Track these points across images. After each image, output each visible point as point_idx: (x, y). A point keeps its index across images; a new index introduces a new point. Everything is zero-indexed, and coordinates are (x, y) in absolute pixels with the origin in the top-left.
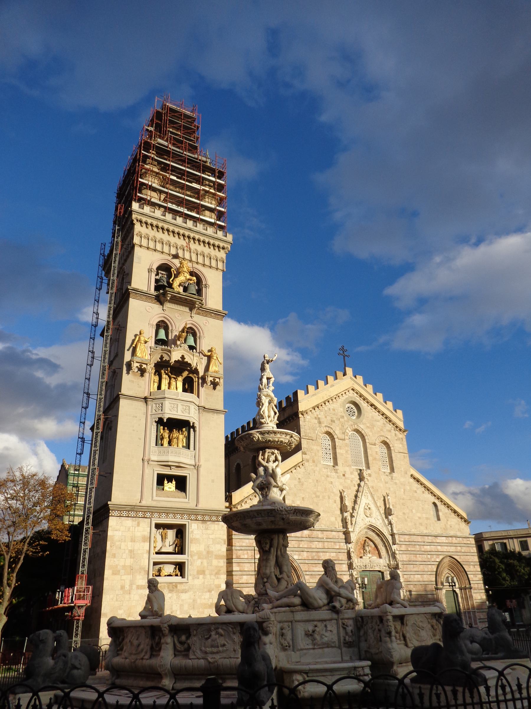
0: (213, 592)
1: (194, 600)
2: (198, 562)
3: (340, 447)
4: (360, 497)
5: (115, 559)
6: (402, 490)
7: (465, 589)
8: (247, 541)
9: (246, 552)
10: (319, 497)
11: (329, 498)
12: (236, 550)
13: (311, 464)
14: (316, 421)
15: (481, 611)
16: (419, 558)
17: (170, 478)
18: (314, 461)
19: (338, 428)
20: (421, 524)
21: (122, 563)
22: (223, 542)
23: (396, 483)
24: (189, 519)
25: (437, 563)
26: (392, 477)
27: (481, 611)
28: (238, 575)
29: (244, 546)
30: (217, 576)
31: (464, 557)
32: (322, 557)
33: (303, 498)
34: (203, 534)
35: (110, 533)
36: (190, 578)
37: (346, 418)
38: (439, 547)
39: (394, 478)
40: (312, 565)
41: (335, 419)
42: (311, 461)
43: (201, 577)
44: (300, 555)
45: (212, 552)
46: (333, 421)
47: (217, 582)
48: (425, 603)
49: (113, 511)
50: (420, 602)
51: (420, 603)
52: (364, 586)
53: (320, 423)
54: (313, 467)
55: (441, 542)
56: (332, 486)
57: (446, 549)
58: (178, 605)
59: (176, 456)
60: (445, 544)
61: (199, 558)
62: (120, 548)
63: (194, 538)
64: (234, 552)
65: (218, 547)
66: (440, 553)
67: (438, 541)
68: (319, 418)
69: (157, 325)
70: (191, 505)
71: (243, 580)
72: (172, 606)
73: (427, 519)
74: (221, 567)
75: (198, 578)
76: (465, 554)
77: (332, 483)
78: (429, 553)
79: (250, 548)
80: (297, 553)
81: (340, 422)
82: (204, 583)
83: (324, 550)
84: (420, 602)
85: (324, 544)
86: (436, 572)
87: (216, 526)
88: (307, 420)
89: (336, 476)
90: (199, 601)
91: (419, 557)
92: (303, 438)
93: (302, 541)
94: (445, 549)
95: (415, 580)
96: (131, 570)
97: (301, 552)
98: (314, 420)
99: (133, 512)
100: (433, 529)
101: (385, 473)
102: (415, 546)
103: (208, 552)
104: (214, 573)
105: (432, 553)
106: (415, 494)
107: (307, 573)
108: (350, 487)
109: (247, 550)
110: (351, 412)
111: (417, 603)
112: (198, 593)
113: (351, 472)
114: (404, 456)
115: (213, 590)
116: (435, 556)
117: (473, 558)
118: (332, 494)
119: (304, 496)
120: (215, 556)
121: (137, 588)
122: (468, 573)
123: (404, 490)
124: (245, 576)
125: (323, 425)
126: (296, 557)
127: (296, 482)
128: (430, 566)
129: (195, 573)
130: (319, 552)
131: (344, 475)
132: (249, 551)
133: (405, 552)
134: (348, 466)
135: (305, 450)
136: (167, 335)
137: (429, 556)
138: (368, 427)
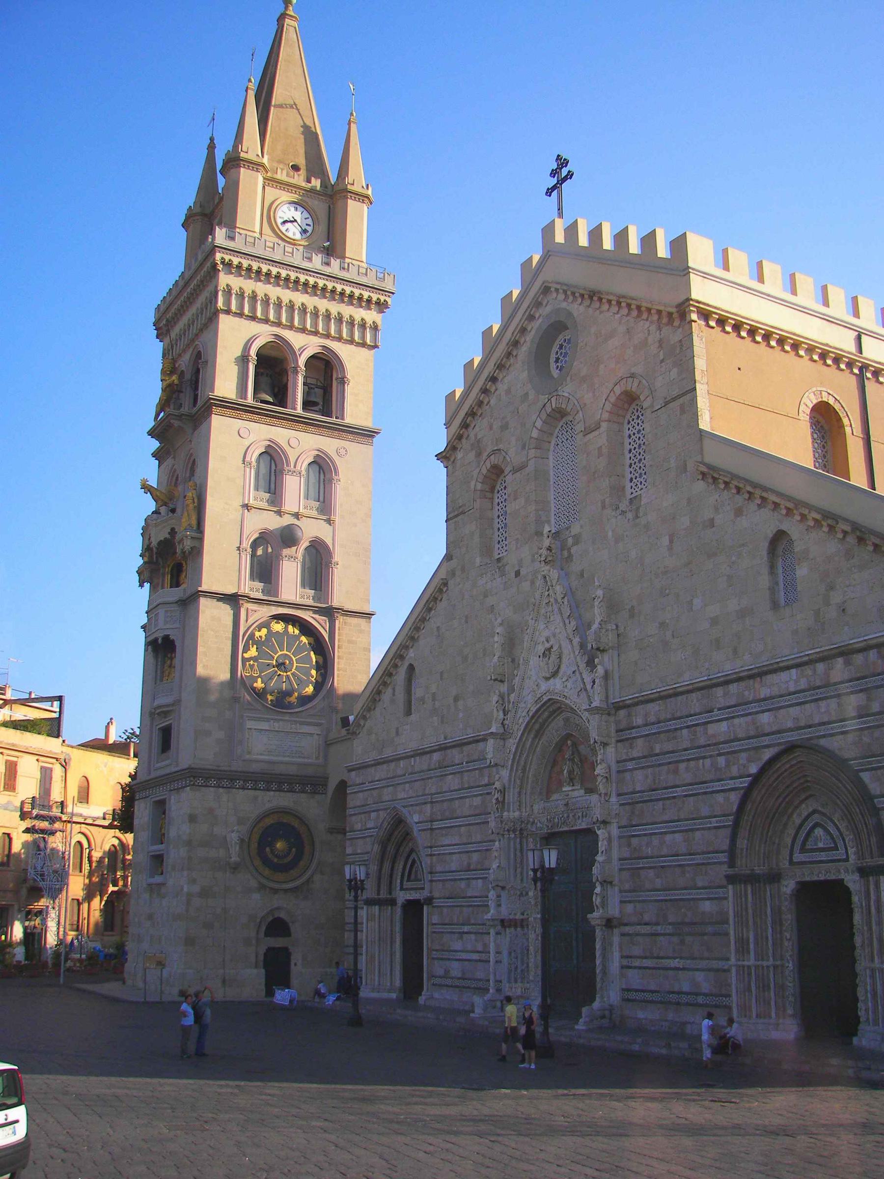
6: (665, 541)
8: (361, 795)
14: (474, 452)
18: (463, 569)
19: (513, 439)
20: (717, 644)
25: (745, 782)
26: (638, 509)
38: (765, 718)
50: (670, 924)
51: (670, 929)
55: (775, 691)
57: (796, 719)
60: (793, 699)
66: (766, 741)
67: (764, 692)
68: (479, 441)
78: (726, 748)
80: (418, 808)
83: (463, 793)
84: (670, 924)
88: (458, 463)
91: (687, 768)
94: (789, 717)
95: (665, 851)
102: (679, 733)
111: (659, 929)
116: (744, 755)
123: (671, 541)
125: (485, 455)
131: (517, 574)
133: (644, 763)
137: (721, 761)
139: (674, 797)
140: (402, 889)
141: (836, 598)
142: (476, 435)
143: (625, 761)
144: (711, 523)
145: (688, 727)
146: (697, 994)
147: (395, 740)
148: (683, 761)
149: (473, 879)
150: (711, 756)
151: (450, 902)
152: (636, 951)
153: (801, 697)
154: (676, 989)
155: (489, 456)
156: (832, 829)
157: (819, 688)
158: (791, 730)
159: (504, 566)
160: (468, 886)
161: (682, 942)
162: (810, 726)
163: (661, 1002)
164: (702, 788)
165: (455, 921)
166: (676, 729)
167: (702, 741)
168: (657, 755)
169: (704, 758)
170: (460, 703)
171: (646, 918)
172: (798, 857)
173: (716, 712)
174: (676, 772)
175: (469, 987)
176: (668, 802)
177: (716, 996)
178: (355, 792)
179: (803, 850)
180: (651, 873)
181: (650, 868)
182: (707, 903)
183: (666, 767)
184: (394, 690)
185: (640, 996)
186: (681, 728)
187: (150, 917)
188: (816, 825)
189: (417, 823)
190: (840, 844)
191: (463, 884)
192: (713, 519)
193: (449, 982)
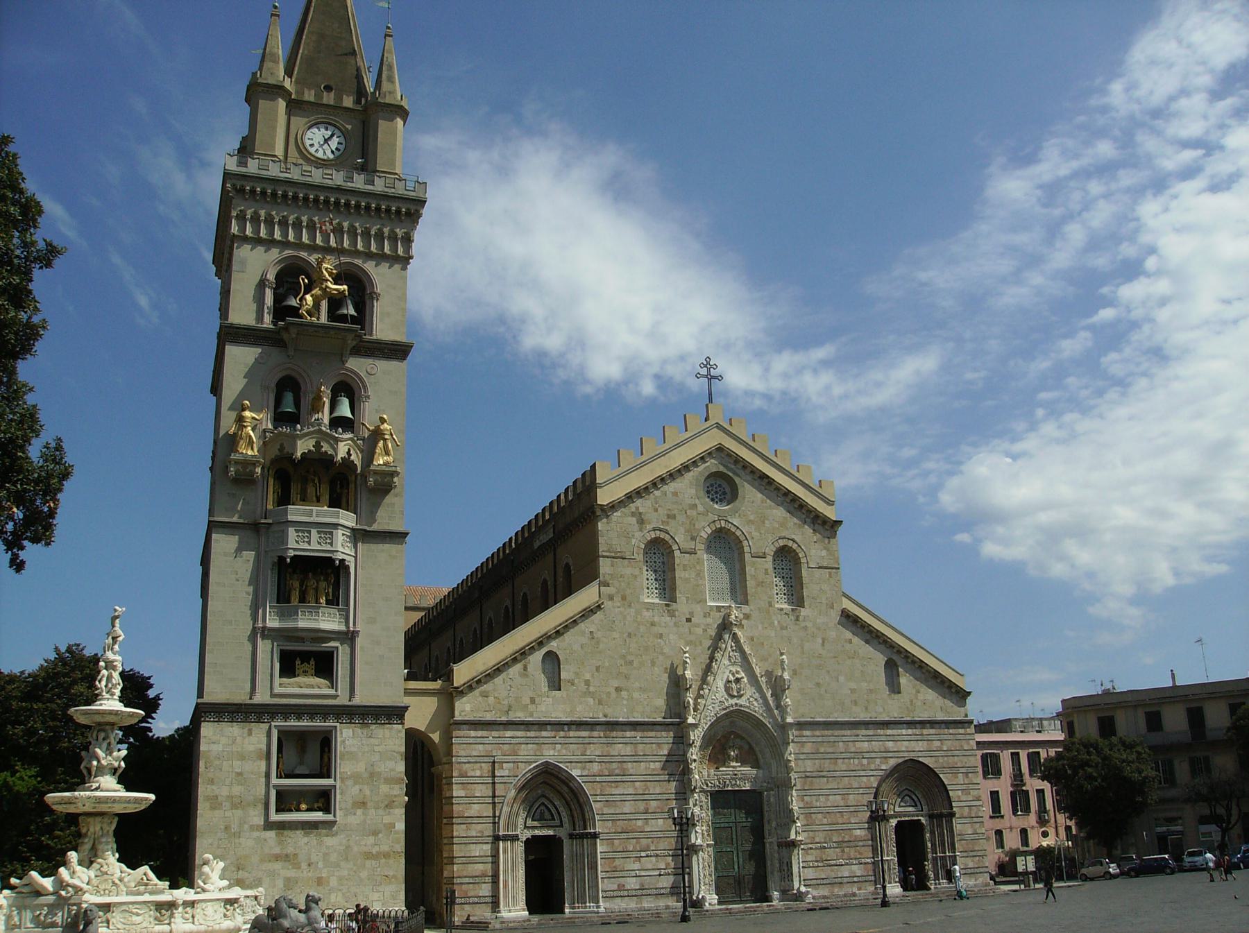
0: (380, 835)
1: (348, 847)
2: (355, 790)
3: (684, 566)
4: (719, 660)
5: (214, 787)
7: (941, 816)
9: (479, 765)
10: (631, 663)
11: (653, 663)
12: (460, 763)
13: (619, 604)
15: (971, 854)
16: (841, 765)
17: (305, 656)
18: (624, 598)
19: (682, 530)
21: (225, 792)
22: (399, 757)
23: (805, 628)
24: (338, 722)
27: (971, 854)
28: (462, 803)
29: (475, 756)
30: (388, 810)
31: (946, 758)
32: (631, 771)
33: (598, 669)
34: (362, 744)
35: (203, 747)
36: (338, 813)
37: (700, 508)
38: (890, 744)
39: (801, 618)
40: (609, 784)
41: (676, 512)
42: (617, 599)
43: (359, 812)
44: (584, 768)
45: (380, 773)
46: (671, 517)
47: (387, 819)
48: (845, 844)
49: (207, 714)
52: (684, 820)
53: (641, 522)
54: (622, 609)
56: (663, 643)
57: (907, 747)
58: (321, 854)
59: (311, 619)
61: (355, 783)
62: (221, 769)
63: (347, 752)
64: (455, 766)
65: (391, 764)
66: (890, 754)
68: (640, 513)
69: (277, 385)
70: (343, 700)
71: (473, 812)
72: (310, 855)
73: (871, 691)
74: (395, 796)
75: (355, 814)
76: (950, 753)
77: (661, 636)
79: (486, 759)
80: (580, 764)
81: (687, 516)
82: (365, 821)
83: (636, 758)
85: (636, 748)
86: (877, 789)
87: (387, 732)
89: (672, 624)
90: (356, 849)
92: (603, 557)
93: (590, 743)
96: (237, 803)
97: (588, 764)
98: (630, 518)
99: (240, 714)
100: (881, 710)
101: (782, 609)
102: (836, 744)
103: (372, 775)
104: (383, 805)
105: (873, 755)
106: (848, 646)
107: (598, 798)
108: (701, 642)
109: (480, 762)
110: (716, 493)
112: (353, 836)
113: (705, 613)
114: (830, 573)
115: (380, 832)
116: (878, 760)
117: (966, 760)
118: (661, 658)
119: (599, 663)
120: (385, 779)
121: (251, 828)
122: (949, 788)
123: (823, 642)
124: (476, 805)
125: (649, 527)
126: (575, 773)
127: (584, 640)
128: (864, 779)
129: (349, 806)
130: (625, 762)
131: (689, 620)
132: (483, 765)
133: (812, 756)
134: (698, 603)
135: (608, 578)
136: (297, 404)
137: (865, 761)
138: (750, 522)
139: (834, 777)
140: (525, 827)
141: (921, 697)
142: (637, 508)
143: (799, 754)
144: (850, 641)
145: (843, 741)
146: (854, 877)
147: (529, 706)
148: (840, 758)
149: (653, 819)
150: (858, 758)
151: (624, 836)
152: (809, 858)
153: (909, 738)
154: (840, 876)
155: (654, 530)
156: (914, 797)
157: (918, 735)
158: (903, 751)
159: (674, 611)
160: (647, 824)
161: (843, 851)
162: (914, 751)
163: (829, 884)
164: (853, 774)
165: (631, 849)
166: (835, 742)
167: (853, 750)
168: (822, 753)
169: (854, 758)
170: (624, 694)
171: (817, 840)
172: (897, 809)
173: (861, 737)
174: (836, 764)
175: (649, 895)
176: (830, 779)
177: (865, 876)
178: (470, 743)
179: (900, 806)
180: (820, 816)
181: (819, 813)
182: (859, 830)
183: (828, 761)
184: (525, 668)
185: (815, 882)
186: (838, 742)
187: (286, 858)
188: (908, 795)
189: (578, 776)
190: (918, 804)
191: (640, 823)
192: (851, 640)
193: (625, 893)
